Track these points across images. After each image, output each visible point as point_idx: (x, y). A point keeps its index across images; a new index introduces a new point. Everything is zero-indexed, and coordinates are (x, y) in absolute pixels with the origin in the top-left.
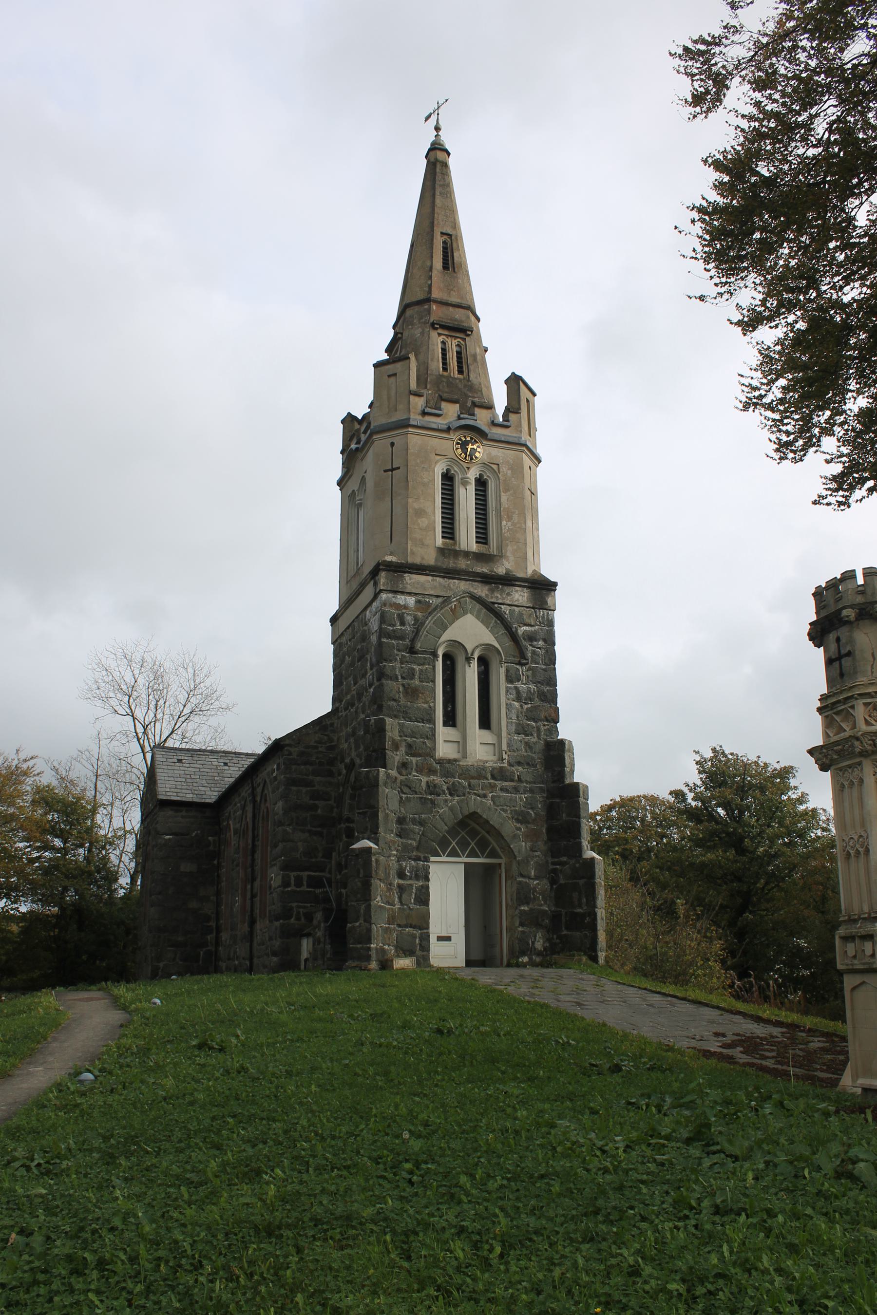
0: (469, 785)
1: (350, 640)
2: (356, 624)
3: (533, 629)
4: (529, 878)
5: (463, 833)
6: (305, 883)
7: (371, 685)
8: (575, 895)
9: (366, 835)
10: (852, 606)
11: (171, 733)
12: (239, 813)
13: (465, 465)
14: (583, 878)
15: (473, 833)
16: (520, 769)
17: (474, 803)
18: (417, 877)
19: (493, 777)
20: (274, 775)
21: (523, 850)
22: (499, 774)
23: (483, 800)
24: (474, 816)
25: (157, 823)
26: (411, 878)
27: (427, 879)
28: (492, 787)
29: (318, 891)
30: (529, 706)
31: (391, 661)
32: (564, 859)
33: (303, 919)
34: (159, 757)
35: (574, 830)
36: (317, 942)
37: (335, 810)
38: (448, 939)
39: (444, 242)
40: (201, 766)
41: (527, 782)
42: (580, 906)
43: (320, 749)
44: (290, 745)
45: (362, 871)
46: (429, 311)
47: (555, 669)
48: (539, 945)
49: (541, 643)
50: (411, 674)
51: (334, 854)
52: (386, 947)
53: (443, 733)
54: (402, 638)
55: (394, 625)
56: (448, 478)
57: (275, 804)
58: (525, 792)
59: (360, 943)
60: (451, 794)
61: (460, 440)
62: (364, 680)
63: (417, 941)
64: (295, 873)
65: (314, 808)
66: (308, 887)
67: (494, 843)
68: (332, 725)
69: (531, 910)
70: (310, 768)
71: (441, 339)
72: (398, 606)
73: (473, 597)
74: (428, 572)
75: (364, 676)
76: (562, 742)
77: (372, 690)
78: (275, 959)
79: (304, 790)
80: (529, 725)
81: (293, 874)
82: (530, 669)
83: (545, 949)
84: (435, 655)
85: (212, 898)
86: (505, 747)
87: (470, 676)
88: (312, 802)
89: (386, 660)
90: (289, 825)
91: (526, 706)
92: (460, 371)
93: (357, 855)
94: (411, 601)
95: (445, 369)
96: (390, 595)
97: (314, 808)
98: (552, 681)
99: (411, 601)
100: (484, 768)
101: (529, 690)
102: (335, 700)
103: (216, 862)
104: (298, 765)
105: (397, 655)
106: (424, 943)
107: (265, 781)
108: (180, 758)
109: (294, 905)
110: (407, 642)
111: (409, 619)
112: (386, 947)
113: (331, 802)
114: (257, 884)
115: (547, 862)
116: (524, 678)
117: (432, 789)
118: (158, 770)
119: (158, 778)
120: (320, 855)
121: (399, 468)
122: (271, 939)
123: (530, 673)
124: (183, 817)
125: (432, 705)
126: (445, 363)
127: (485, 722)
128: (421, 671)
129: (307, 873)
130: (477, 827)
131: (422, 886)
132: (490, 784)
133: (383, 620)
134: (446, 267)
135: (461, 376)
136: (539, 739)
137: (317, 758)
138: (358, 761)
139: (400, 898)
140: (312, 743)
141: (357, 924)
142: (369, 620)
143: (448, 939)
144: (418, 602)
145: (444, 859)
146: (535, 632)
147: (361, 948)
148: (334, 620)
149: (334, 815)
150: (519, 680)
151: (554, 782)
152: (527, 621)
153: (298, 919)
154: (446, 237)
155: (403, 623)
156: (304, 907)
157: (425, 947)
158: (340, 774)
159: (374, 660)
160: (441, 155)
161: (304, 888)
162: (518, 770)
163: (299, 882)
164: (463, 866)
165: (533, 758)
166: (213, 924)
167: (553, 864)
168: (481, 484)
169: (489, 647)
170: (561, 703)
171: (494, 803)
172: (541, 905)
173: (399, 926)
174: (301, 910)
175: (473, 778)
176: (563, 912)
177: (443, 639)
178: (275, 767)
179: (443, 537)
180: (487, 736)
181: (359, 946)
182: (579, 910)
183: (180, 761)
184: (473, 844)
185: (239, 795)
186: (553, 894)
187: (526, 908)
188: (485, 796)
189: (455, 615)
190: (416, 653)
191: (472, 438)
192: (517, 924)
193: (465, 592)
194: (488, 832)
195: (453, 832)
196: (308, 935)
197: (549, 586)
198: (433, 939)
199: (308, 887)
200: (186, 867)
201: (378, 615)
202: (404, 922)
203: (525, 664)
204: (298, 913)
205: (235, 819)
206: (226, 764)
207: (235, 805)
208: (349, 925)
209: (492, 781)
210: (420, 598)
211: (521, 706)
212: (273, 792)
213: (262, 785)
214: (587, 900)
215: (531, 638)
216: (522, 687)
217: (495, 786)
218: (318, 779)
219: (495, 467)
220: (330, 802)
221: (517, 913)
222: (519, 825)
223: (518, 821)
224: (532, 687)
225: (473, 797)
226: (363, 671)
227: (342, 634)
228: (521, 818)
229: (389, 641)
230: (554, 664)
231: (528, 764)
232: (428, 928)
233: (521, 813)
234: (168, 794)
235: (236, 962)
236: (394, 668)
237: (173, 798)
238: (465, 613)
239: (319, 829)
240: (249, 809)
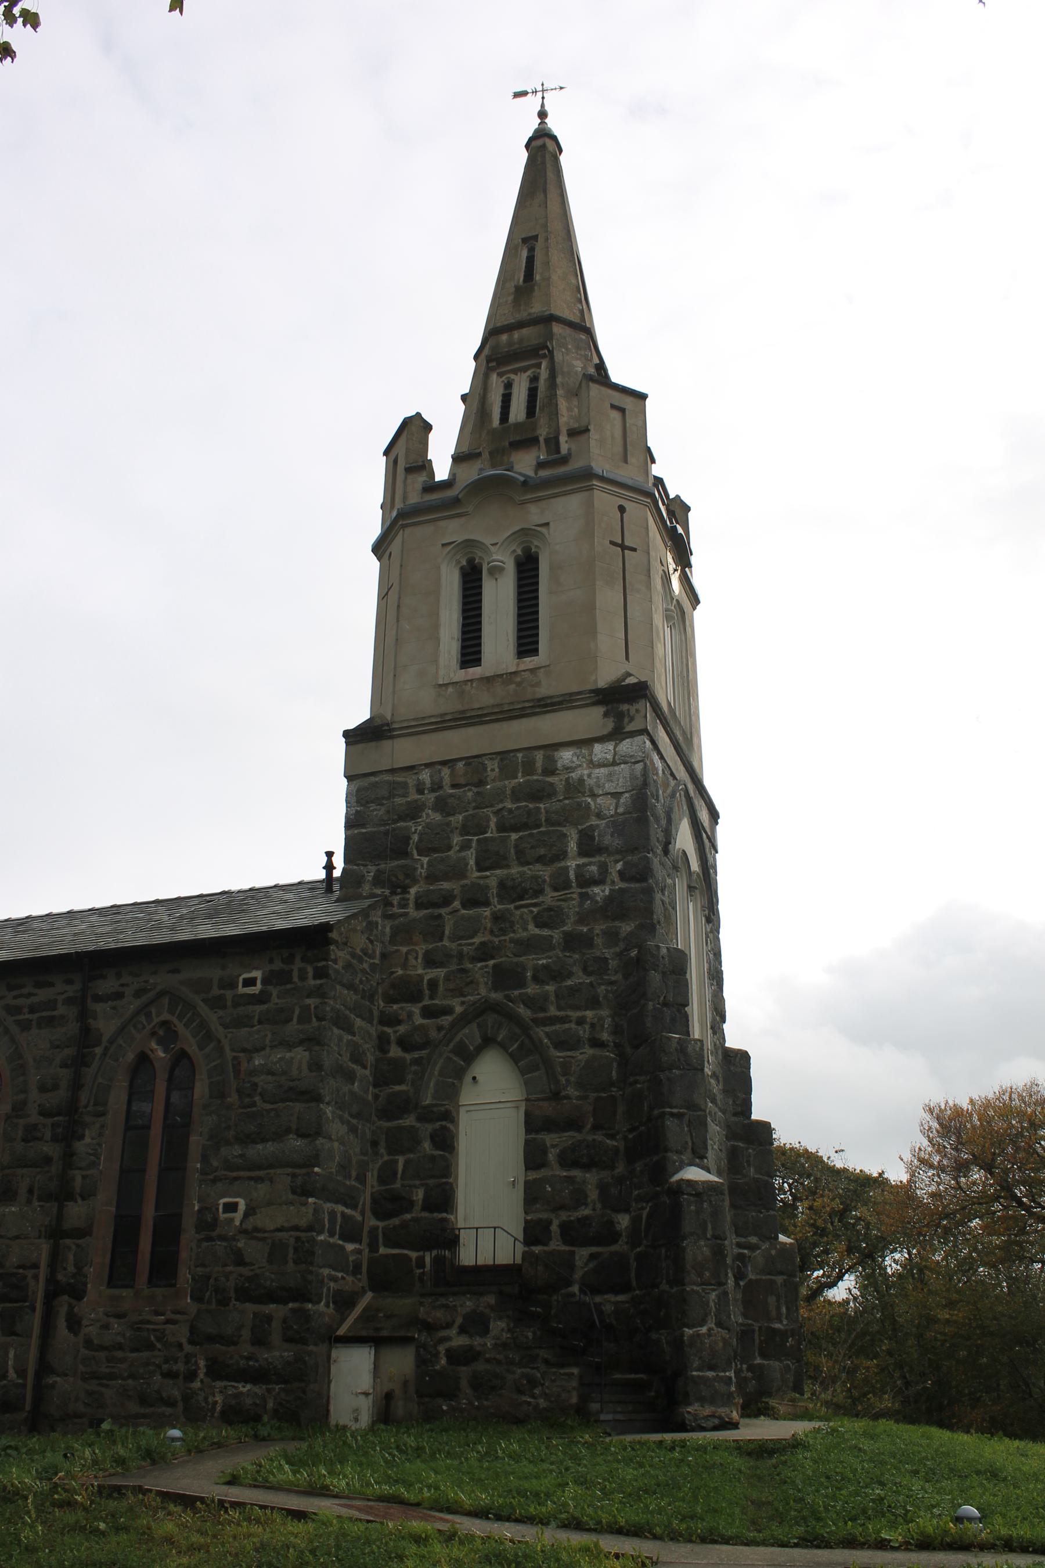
8: (772, 1300)
14: (781, 1273)
32: (753, 1240)
45: (710, 1227)
90: (328, 1104)
93: (698, 1195)
167: (739, 1245)
176: (756, 1326)
182: (777, 1326)
186: (739, 1296)
214: (788, 1309)
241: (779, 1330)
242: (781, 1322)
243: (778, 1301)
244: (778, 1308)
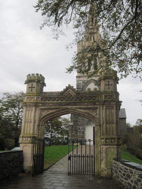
18: (82, 130)
72: (79, 83)
73: (93, 80)
94: (82, 82)
99: (82, 82)
110: (81, 89)
111: (81, 85)
155: (80, 86)
164: (93, 127)
177: (87, 88)
189: (90, 83)
238: (92, 83)
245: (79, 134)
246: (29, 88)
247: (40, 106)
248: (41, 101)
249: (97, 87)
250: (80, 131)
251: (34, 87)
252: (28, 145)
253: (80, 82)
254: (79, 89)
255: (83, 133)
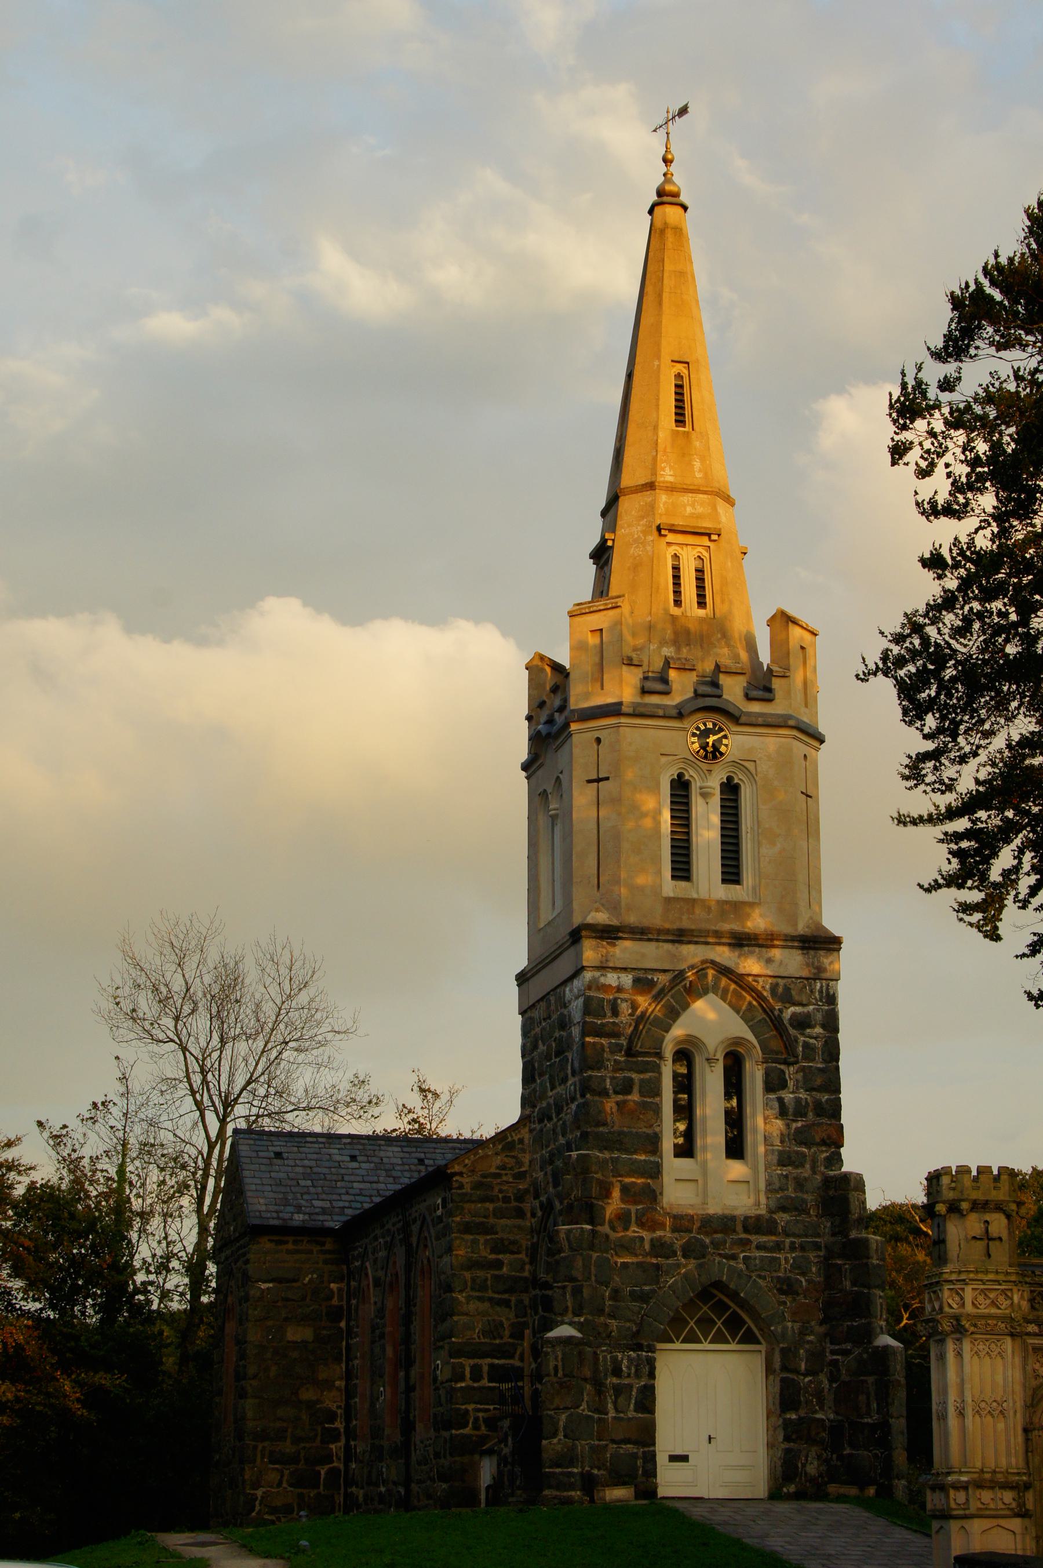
0: (712, 1243)
1: (544, 1019)
2: (552, 999)
3: (805, 1010)
4: (797, 1372)
5: (705, 1308)
6: (485, 1376)
7: (573, 1099)
9: (566, 1319)
10: (944, 1202)
11: (248, 1083)
12: (382, 1254)
13: (705, 767)
15: (720, 1308)
16: (786, 1217)
17: (720, 1268)
18: (638, 1375)
19: (746, 1230)
20: (439, 1213)
21: (790, 1333)
22: (754, 1225)
23: (732, 1263)
24: (718, 1285)
25: (247, 1262)
26: (629, 1376)
27: (652, 1375)
28: (745, 1243)
29: (505, 1386)
30: (799, 1124)
31: (599, 1069)
33: (483, 1428)
34: (244, 1149)
35: (860, 1306)
36: (502, 1461)
37: (527, 1267)
38: (684, 1458)
39: (679, 376)
40: (313, 1163)
41: (794, 1235)
42: (868, 1414)
43: (504, 1178)
44: (461, 1174)
46: (652, 507)
47: (837, 1068)
48: (812, 1469)
49: (818, 1030)
50: (626, 1088)
51: (527, 1332)
52: (595, 1471)
53: (673, 1166)
54: (616, 1035)
55: (605, 1016)
56: (681, 788)
57: (440, 1257)
58: (793, 1248)
59: (558, 1466)
60: (684, 1256)
61: (698, 728)
62: (563, 1087)
63: (639, 1462)
64: (472, 1362)
65: (498, 1264)
66: (490, 1381)
67: (750, 1323)
68: (521, 1141)
69: (800, 1419)
70: (490, 1206)
71: (672, 550)
72: (606, 988)
74: (650, 936)
75: (564, 1080)
76: (846, 1177)
77: (573, 1106)
78: (444, 1486)
79: (482, 1239)
80: (797, 1152)
81: (468, 1363)
82: (803, 1069)
83: (821, 1475)
84: (659, 1055)
85: (337, 1383)
86: (762, 1186)
87: (711, 1083)
88: (493, 1256)
89: (592, 1069)
90: (461, 1291)
91: (794, 1125)
92: (702, 604)
95: (678, 603)
96: (597, 974)
97: (498, 1264)
98: (832, 1084)
99: (627, 980)
100: (733, 1218)
101: (798, 1100)
102: (526, 1101)
103: (343, 1324)
104: (473, 1202)
105: (608, 1060)
106: (649, 1466)
107: (424, 1218)
108: (278, 1149)
109: (471, 1407)
110: (624, 1042)
111: (624, 1008)
112: (595, 1471)
113: (522, 1256)
114: (414, 1372)
115: (824, 1349)
116: (791, 1084)
117: (660, 1248)
118: (246, 1173)
119: (247, 1187)
120: (507, 1333)
121: (607, 779)
122: (437, 1455)
123: (800, 1076)
124: (288, 1252)
125: (657, 1129)
126: (677, 593)
127: (735, 1149)
128: (642, 1081)
129: (489, 1360)
130: (725, 1299)
131: (645, 1386)
132: (741, 1239)
133: (587, 1010)
134: (680, 421)
135: (701, 612)
136: (814, 1173)
137: (501, 1191)
138: (558, 1206)
139: (615, 1403)
140: (493, 1170)
141: (555, 1441)
142: (569, 1002)
143: (684, 1458)
144: (636, 981)
145: (678, 1345)
146: (808, 1015)
147: (561, 1473)
148: (522, 978)
149: (526, 1274)
150: (784, 1085)
151: (833, 1235)
152: (796, 998)
153: (476, 1427)
154: (680, 368)
155: (615, 1012)
156: (488, 1410)
157: (651, 1472)
158: (533, 1215)
159: (576, 1065)
160: (671, 212)
161: (485, 1382)
162: (782, 1218)
163: (476, 1375)
165: (804, 1201)
166: (339, 1425)
168: (731, 790)
169: (738, 1041)
170: (846, 1118)
171: (747, 1268)
172: (816, 1412)
173: (613, 1441)
174: (481, 1415)
175: (716, 1232)
178: (439, 1201)
179: (673, 877)
180: (737, 1169)
181: (558, 1470)
183: (278, 1155)
184: (719, 1323)
185: (383, 1226)
187: (794, 1417)
188: (734, 1257)
190: (634, 1056)
191: (715, 725)
192: (781, 1438)
193: (703, 962)
194: (742, 1307)
195: (690, 1305)
196: (490, 1452)
197: (832, 943)
198: (662, 1459)
199: (490, 1381)
200: (296, 1334)
201: (581, 1000)
202: (621, 1436)
203: (792, 1064)
204: (476, 1419)
205: (375, 1261)
206: (353, 1158)
207: (376, 1238)
208: (544, 1442)
209: (743, 1236)
210: (641, 975)
211: (788, 1126)
212: (438, 1238)
213: (419, 1223)
214: (878, 1404)
215: (802, 1023)
216: (788, 1096)
217: (748, 1242)
218: (503, 1221)
219: (750, 766)
220: (520, 1256)
221: (781, 1421)
222: (783, 1298)
223: (781, 1291)
224: (803, 1095)
225: (717, 1259)
226: (562, 1075)
227: (533, 1005)
228: (787, 1287)
229: (597, 1039)
230: (837, 1060)
231: (796, 1209)
232: (654, 1444)
233: (787, 1281)
234: (264, 1215)
235: (383, 1489)
236: (603, 1079)
237: (272, 1222)
239: (506, 1296)
240: (400, 1258)
241: (868, 1423)
242: (871, 1417)
243: (868, 1398)
244: (868, 1405)
245: (612, 1414)
246: (974, 1238)
247: (1028, 1334)
248: (1033, 1308)
249: (750, 1036)
250: (618, 1390)
251: (995, 1235)
252: (1002, 1522)
253: (611, 979)
254: (604, 1041)
255: (647, 1401)
